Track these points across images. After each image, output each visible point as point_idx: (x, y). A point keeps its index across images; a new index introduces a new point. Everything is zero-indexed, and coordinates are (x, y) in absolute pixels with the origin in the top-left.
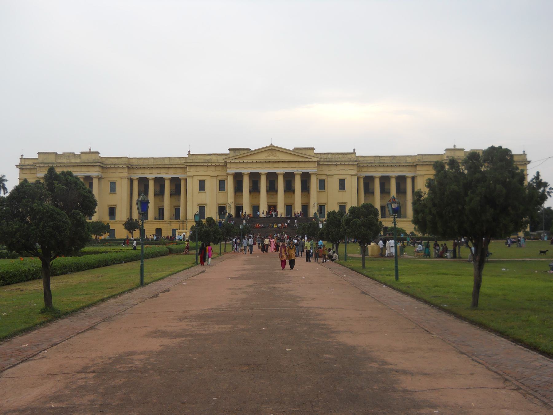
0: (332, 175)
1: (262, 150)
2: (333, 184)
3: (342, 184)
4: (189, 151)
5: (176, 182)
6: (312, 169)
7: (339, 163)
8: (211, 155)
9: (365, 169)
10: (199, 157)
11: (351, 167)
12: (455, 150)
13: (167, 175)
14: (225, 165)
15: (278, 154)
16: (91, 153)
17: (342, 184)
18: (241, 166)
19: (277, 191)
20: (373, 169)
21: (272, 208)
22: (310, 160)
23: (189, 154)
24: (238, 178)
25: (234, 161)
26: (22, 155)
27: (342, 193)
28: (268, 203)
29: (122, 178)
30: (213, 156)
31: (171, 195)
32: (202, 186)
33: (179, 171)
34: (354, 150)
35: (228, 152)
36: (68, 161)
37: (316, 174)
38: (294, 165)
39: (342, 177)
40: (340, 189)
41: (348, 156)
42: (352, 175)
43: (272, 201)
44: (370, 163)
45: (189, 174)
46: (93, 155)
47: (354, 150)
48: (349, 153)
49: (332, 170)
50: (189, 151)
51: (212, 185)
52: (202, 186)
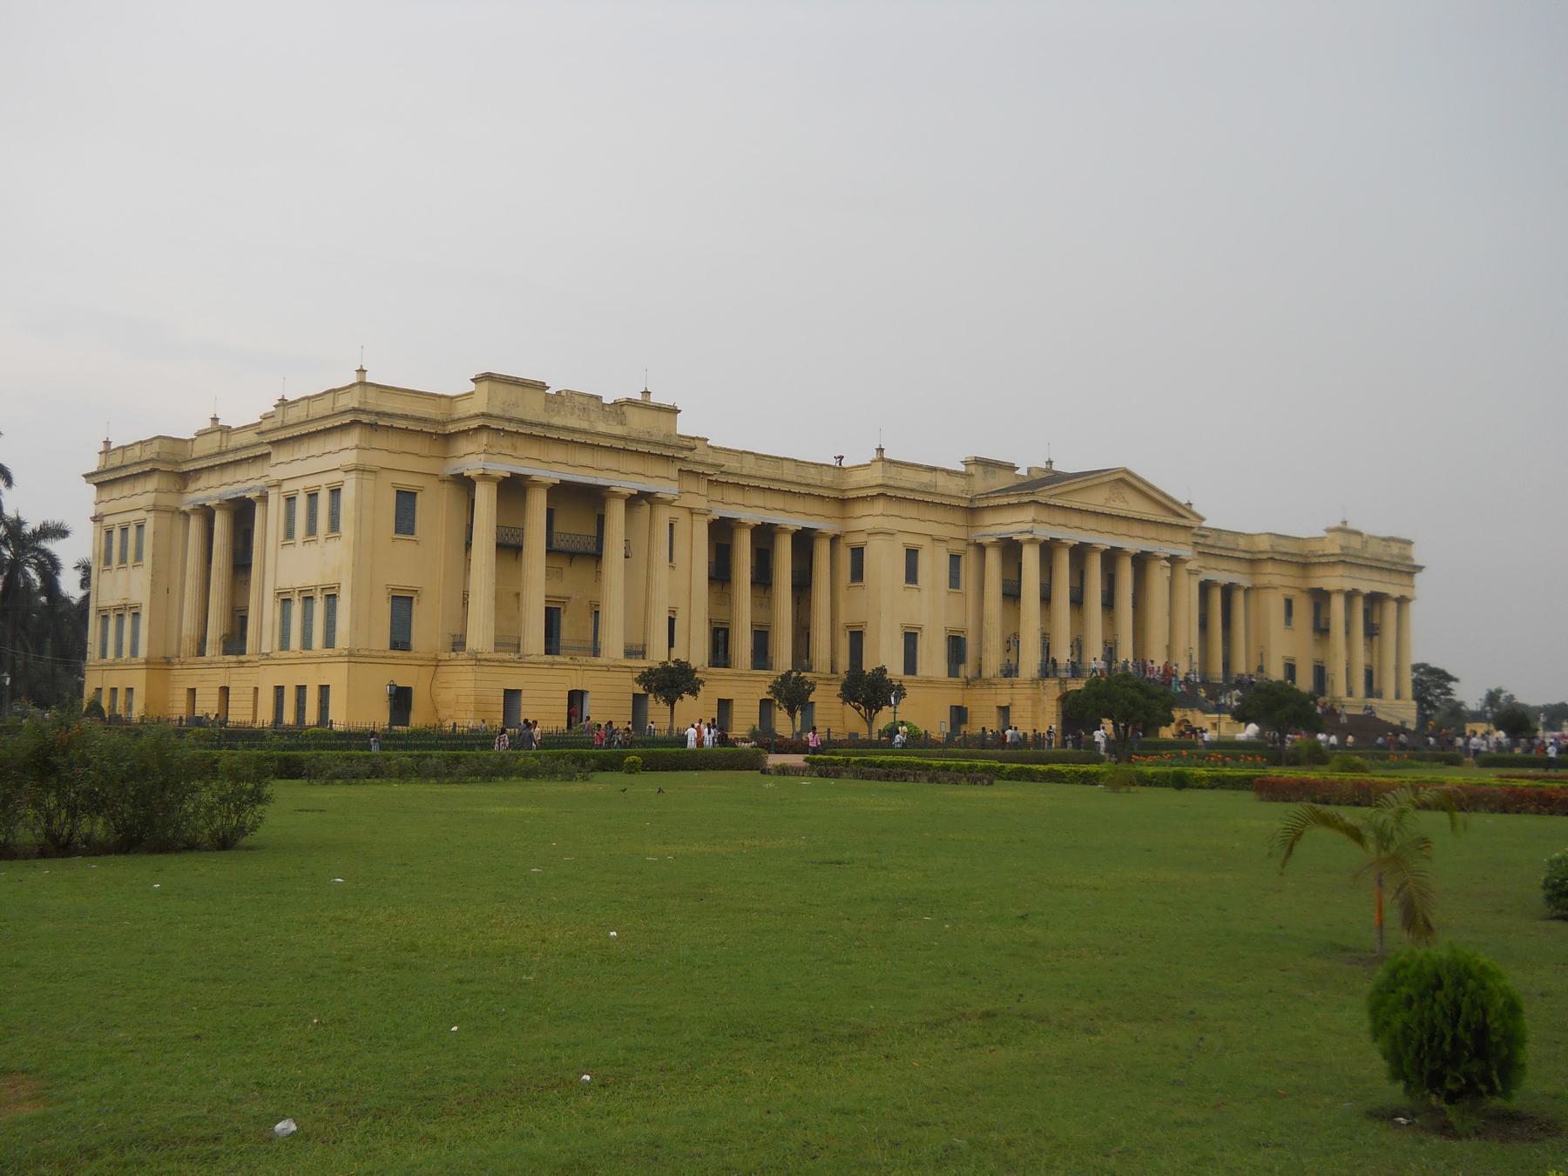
8: (934, 469)
12: (1343, 530)
13: (792, 519)
14: (972, 511)
15: (1130, 496)
16: (644, 405)
26: (362, 371)
29: (692, 511)
31: (754, 583)
35: (962, 468)
36: (584, 425)
46: (664, 416)
50: (881, 450)
51: (933, 565)
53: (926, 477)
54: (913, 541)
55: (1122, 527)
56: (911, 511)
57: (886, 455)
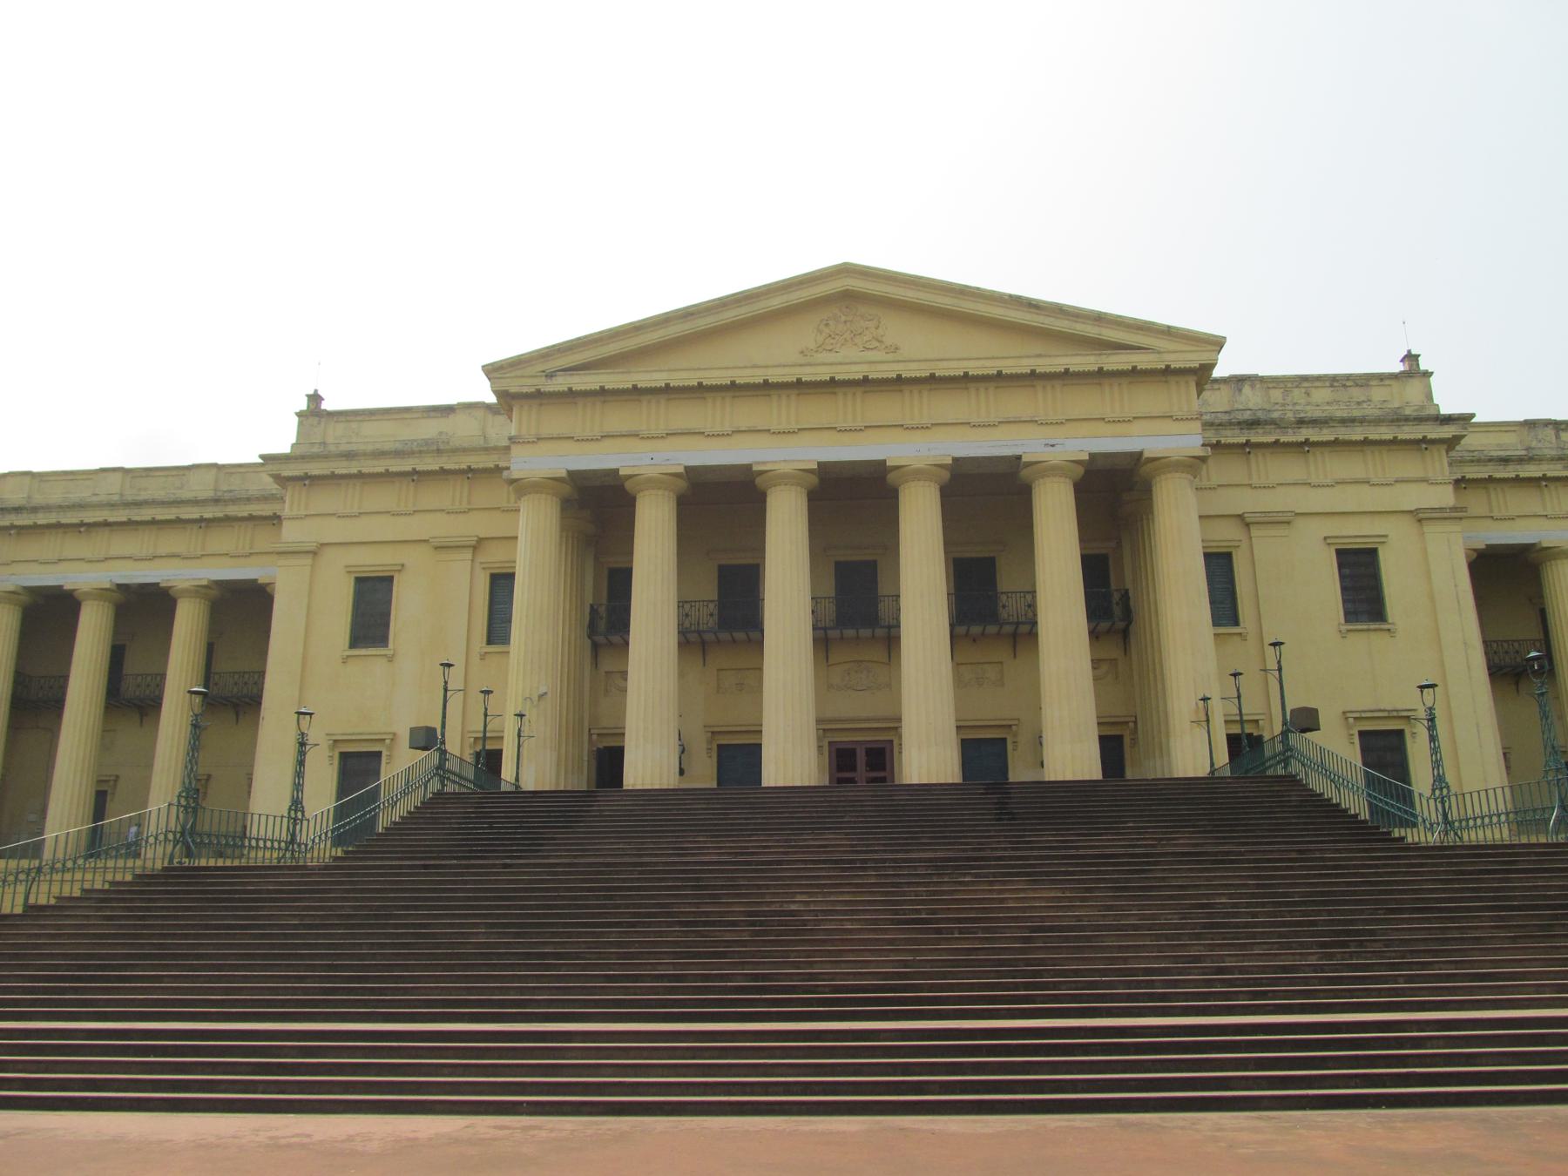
0: (1281, 521)
1: (776, 302)
2: (1295, 585)
3: (1362, 584)
4: (315, 398)
5: (242, 610)
6: (1159, 432)
7: (1326, 435)
8: (447, 410)
9: (1476, 502)
10: (370, 429)
11: (1407, 465)
15: (895, 329)
17: (1362, 584)
18: (619, 418)
19: (891, 641)
20: (1527, 501)
21: (861, 758)
22: (1143, 361)
23: (314, 413)
24: (597, 509)
25: (561, 384)
27: (1365, 642)
28: (824, 726)
30: (459, 418)
32: (371, 616)
33: (263, 539)
34: (1411, 358)
37: (1193, 465)
38: (1017, 403)
39: (1356, 532)
40: (1351, 615)
41: (1378, 393)
42: (1420, 517)
43: (857, 707)
44: (1505, 461)
45: (291, 533)
47: (1411, 358)
48: (1381, 377)
49: (1278, 485)
50: (315, 398)
51: (436, 607)
52: (371, 616)
53: (429, 430)
54: (373, 561)
55: (884, 408)
56: (383, 497)
57: (325, 406)
